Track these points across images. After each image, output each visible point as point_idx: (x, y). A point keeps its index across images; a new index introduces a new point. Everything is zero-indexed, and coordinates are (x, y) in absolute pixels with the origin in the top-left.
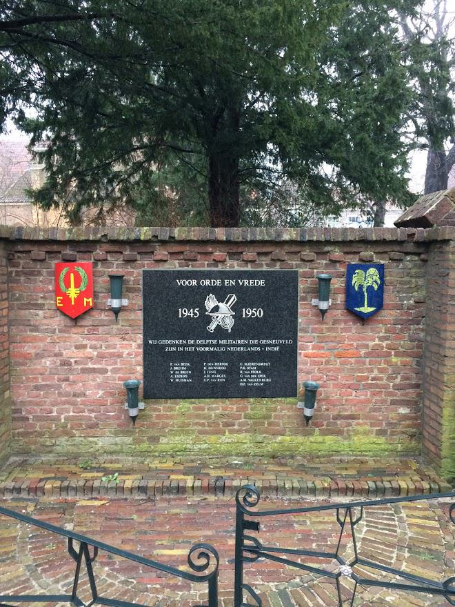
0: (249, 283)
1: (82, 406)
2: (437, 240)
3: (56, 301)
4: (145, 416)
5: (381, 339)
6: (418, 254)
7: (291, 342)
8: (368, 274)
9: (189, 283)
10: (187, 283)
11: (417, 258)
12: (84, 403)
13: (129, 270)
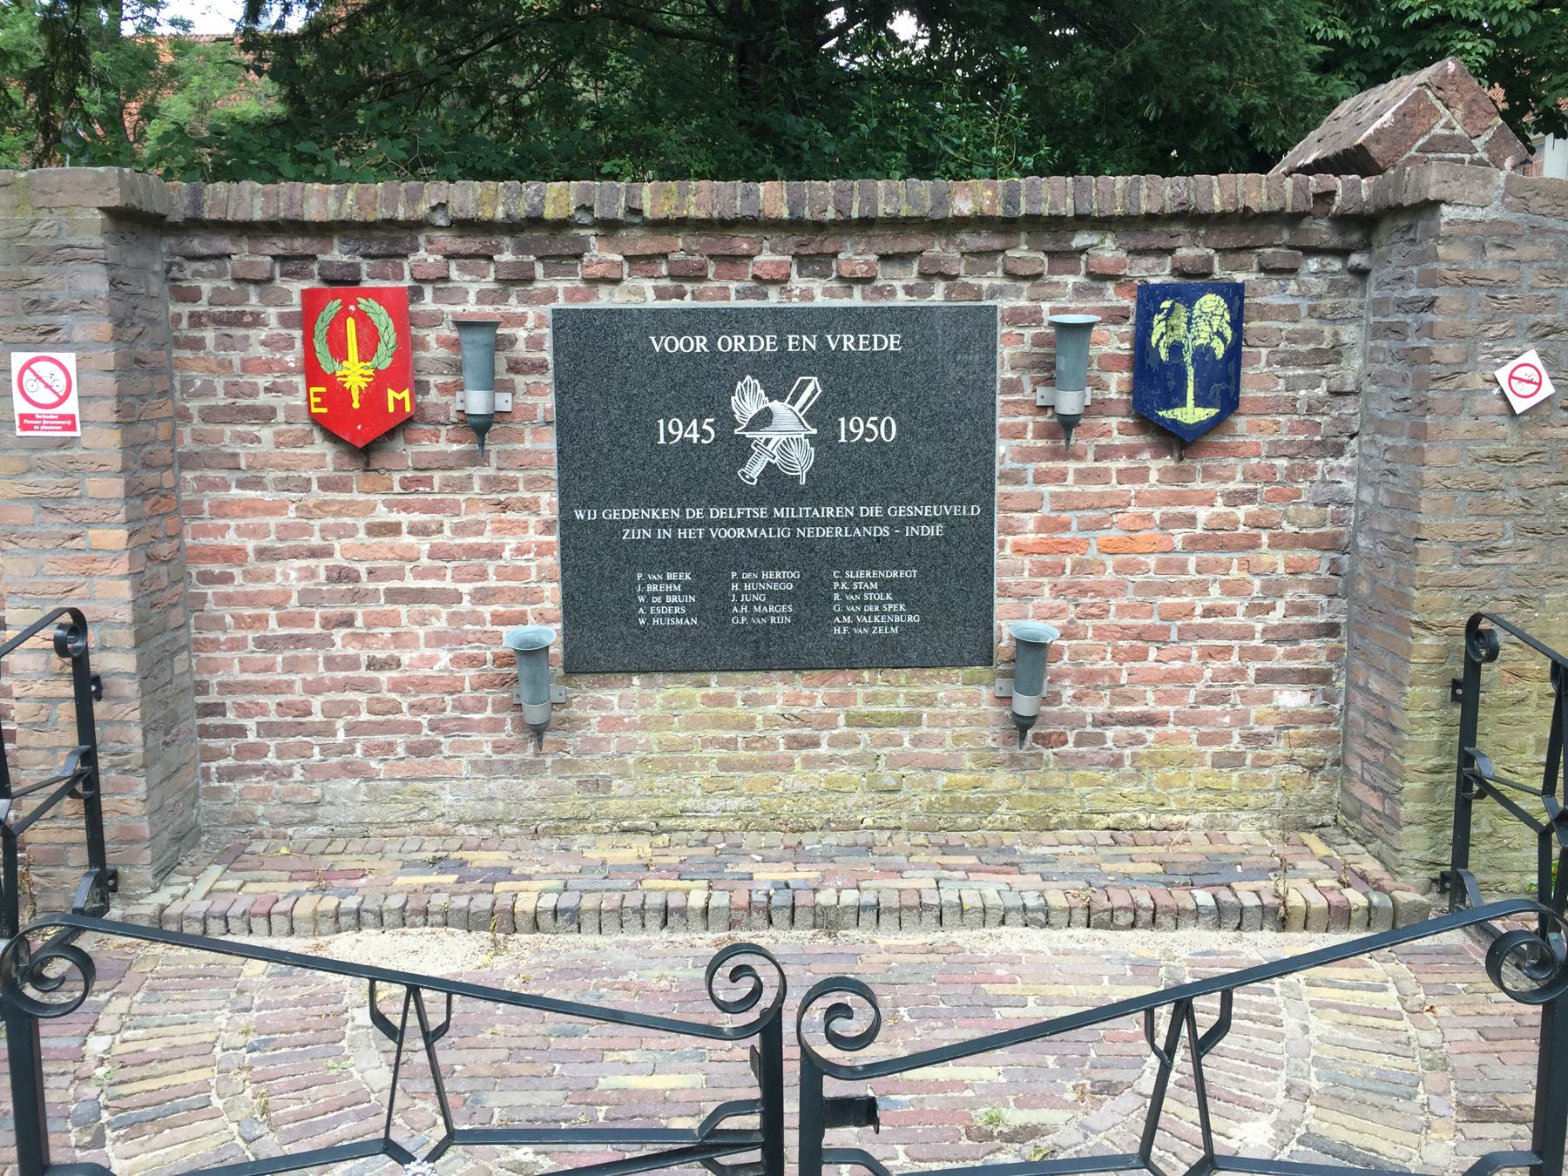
0: (856, 344)
1: (394, 696)
2: (1400, 205)
3: (308, 399)
4: (571, 721)
5: (1234, 499)
6: (1342, 253)
7: (976, 510)
8: (1196, 313)
9: (687, 345)
10: (679, 344)
11: (1336, 265)
12: (396, 687)
13: (513, 310)
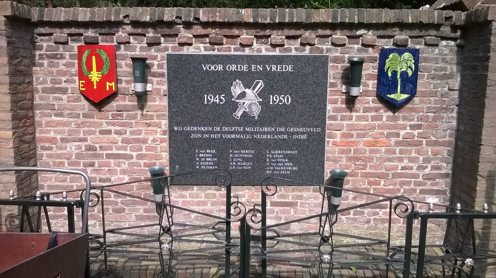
3: (79, 85)
5: (412, 127)
7: (319, 130)
9: (215, 68)
10: (213, 68)
13: (153, 54)
